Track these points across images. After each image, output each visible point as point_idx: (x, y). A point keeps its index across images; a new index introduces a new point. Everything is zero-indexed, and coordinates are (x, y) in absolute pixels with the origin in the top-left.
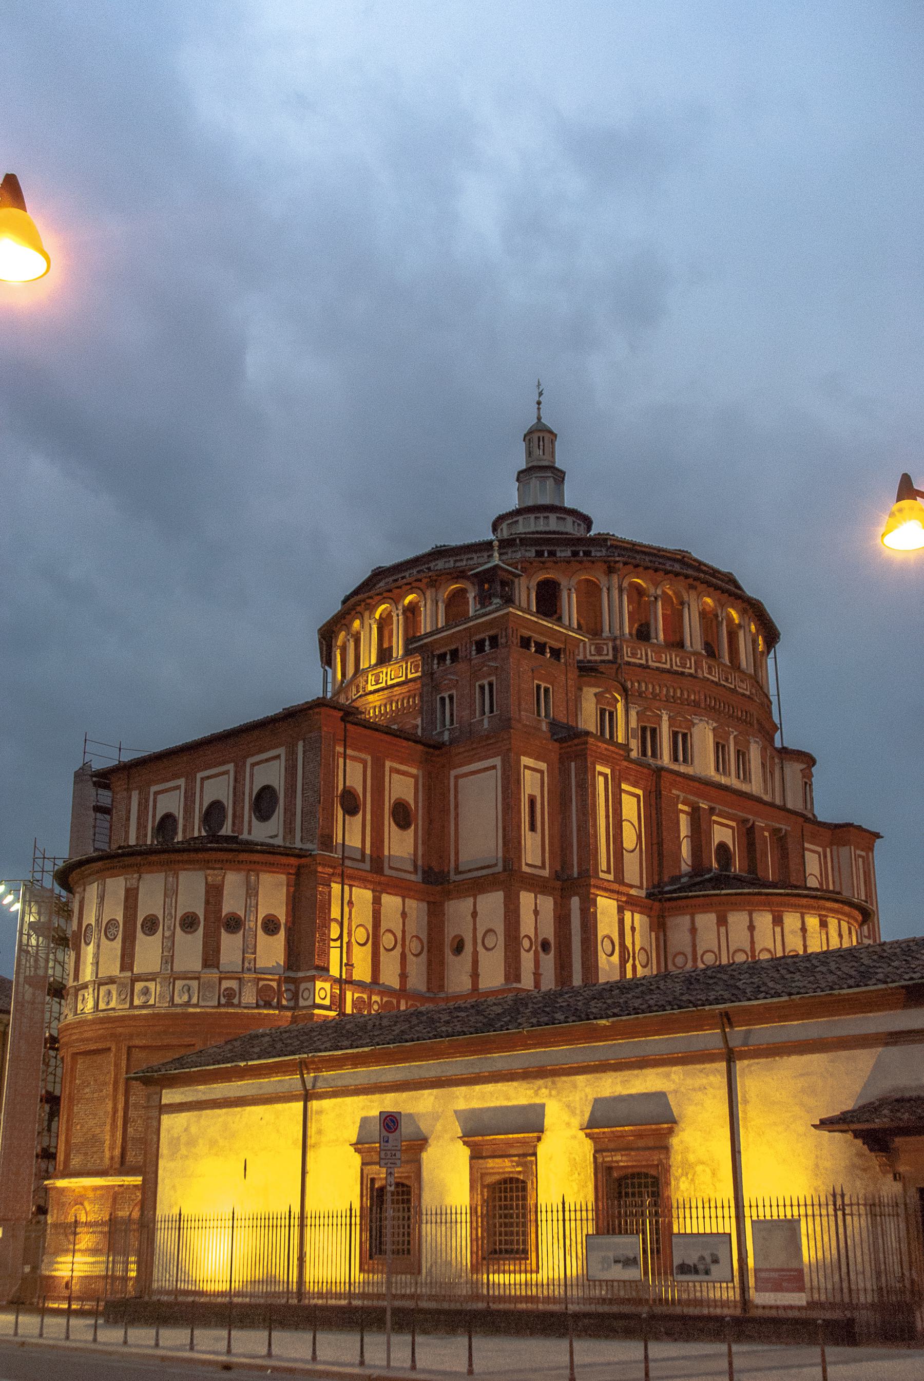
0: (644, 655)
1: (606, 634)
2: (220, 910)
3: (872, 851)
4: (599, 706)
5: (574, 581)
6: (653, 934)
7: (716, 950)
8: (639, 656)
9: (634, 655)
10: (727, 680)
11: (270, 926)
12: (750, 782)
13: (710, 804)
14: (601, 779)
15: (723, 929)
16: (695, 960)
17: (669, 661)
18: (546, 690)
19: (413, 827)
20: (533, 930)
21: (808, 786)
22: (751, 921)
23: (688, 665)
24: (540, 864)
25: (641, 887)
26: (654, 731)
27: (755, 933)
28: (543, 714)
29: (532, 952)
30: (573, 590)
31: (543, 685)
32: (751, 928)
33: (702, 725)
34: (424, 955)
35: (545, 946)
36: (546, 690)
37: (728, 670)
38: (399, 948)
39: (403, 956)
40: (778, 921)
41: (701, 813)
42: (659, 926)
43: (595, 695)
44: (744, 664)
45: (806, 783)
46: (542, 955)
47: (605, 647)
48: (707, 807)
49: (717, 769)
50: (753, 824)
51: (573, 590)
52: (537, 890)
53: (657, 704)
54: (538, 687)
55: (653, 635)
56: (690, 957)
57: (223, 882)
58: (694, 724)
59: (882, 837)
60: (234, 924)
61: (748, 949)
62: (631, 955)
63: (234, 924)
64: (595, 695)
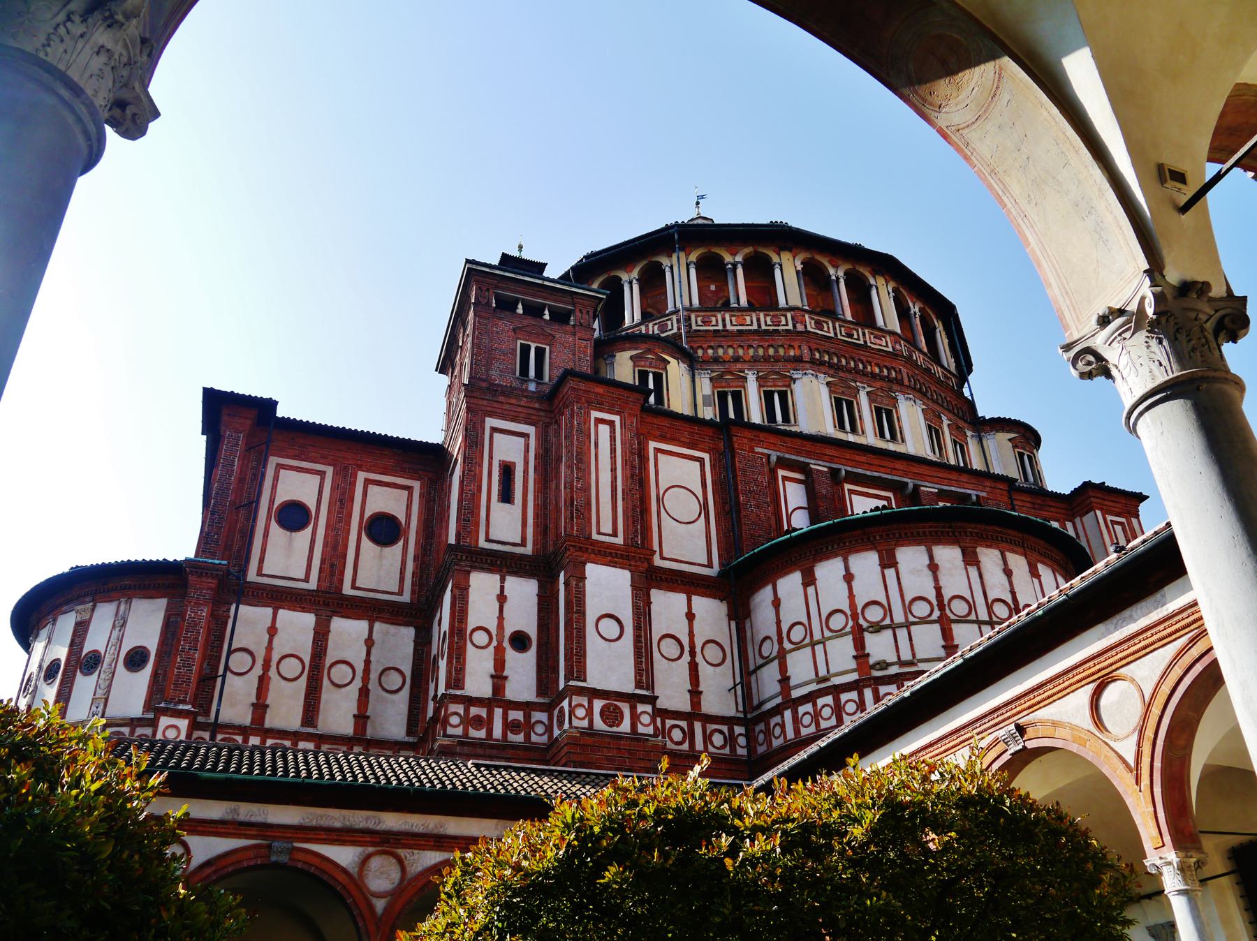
0: (719, 321)
1: (671, 308)
2: (82, 649)
3: (1137, 516)
4: (637, 369)
5: (635, 274)
6: (733, 624)
7: (805, 621)
8: (714, 323)
9: (705, 323)
10: (851, 336)
11: (136, 659)
12: (903, 441)
13: (828, 464)
14: (604, 430)
15: (811, 590)
16: (780, 641)
17: (752, 321)
18: (540, 353)
19: (401, 543)
20: (495, 622)
21: (1026, 457)
22: (847, 568)
23: (784, 322)
24: (518, 540)
25: (710, 565)
26: (737, 397)
27: (854, 584)
28: (532, 373)
29: (491, 648)
30: (634, 281)
31: (533, 346)
32: (849, 578)
33: (806, 379)
34: (405, 692)
35: (520, 642)
36: (540, 353)
37: (852, 326)
38: (358, 683)
39: (364, 693)
40: (888, 562)
41: (814, 476)
42: (740, 613)
43: (632, 358)
44: (880, 322)
45: (1021, 455)
46: (511, 654)
47: (669, 323)
48: (825, 469)
49: (841, 426)
50: (916, 487)
51: (634, 281)
52: (505, 570)
53: (739, 366)
54: (525, 350)
55: (732, 300)
56: (775, 638)
57: (90, 619)
58: (795, 380)
59: (1147, 497)
60: (92, 663)
61: (845, 607)
62: (687, 649)
63: (92, 663)
64: (632, 358)
